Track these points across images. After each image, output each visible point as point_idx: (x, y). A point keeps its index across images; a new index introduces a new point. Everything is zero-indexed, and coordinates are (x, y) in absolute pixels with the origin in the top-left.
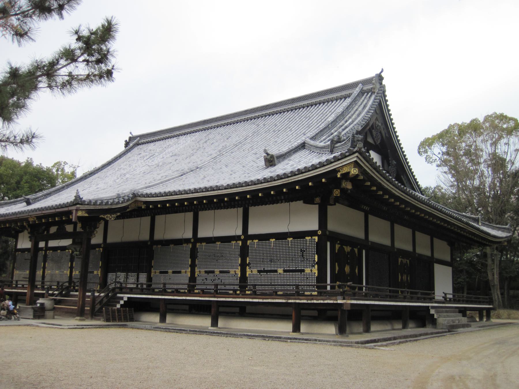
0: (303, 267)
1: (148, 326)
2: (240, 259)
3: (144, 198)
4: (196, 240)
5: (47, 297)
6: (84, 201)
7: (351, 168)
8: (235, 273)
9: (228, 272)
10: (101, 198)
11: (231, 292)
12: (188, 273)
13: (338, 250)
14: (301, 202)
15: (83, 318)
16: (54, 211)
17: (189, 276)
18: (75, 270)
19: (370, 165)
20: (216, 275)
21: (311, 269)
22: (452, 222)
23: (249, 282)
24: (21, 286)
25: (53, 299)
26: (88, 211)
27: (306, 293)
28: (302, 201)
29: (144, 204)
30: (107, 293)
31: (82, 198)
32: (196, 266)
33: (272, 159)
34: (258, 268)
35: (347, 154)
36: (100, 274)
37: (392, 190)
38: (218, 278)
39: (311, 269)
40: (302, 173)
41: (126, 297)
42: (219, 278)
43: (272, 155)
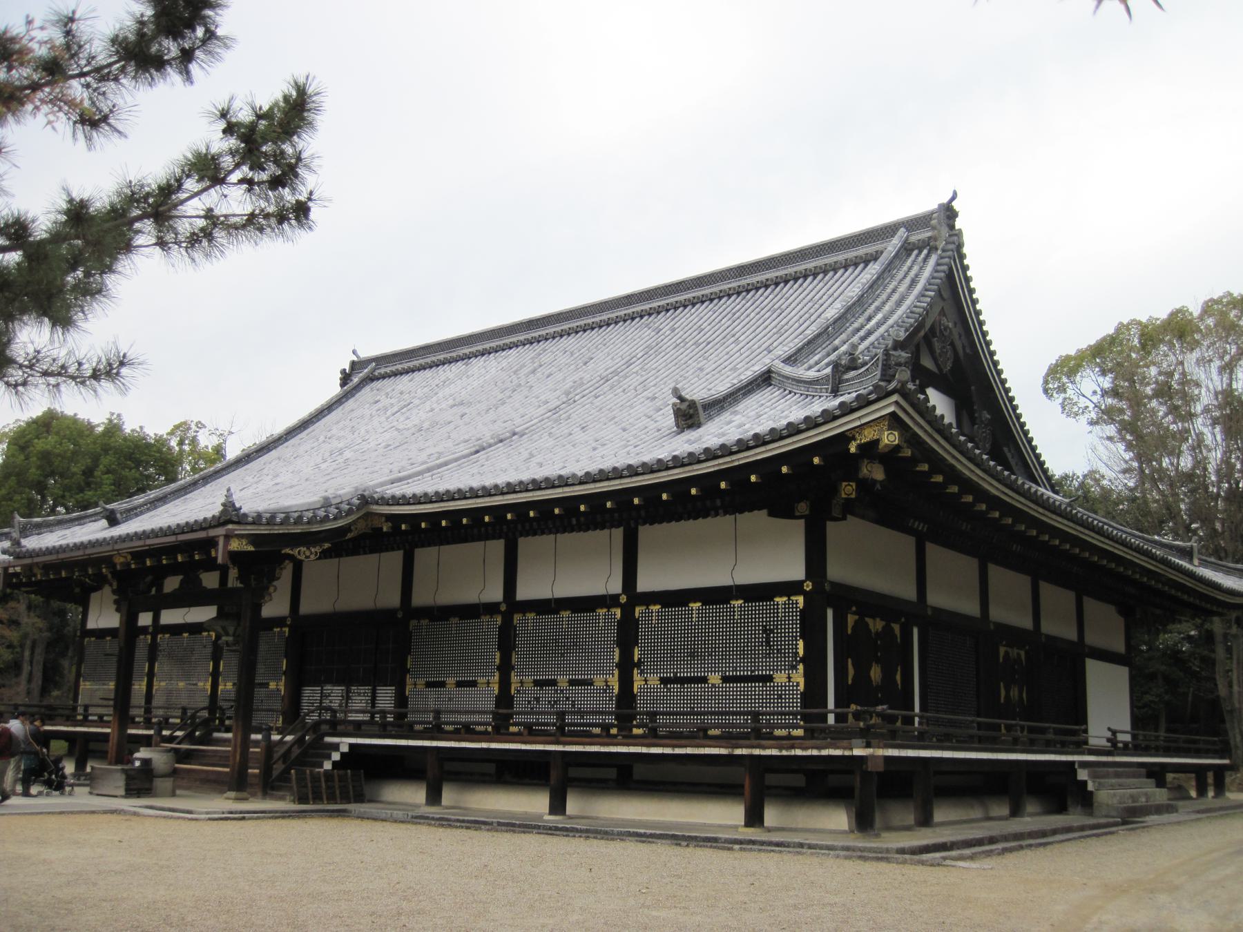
0: (770, 670)
1: (399, 814)
2: (617, 651)
3: (387, 508)
4: (512, 605)
5: (157, 745)
6: (245, 515)
7: (881, 431)
8: (607, 685)
9: (590, 683)
10: (285, 508)
11: (597, 730)
12: (494, 685)
13: (853, 627)
14: (761, 516)
15: (245, 794)
16: (172, 539)
17: (496, 692)
18: (225, 681)
19: (929, 422)
20: (560, 690)
21: (789, 674)
22: (1129, 557)
23: (640, 706)
24: (95, 718)
25: (172, 749)
26: (254, 539)
27: (778, 732)
28: (765, 512)
29: (386, 521)
30: (299, 734)
31: (240, 508)
32: (513, 668)
33: (691, 411)
34: (660, 673)
35: (873, 397)
36: (282, 688)
37: (981, 482)
38: (566, 697)
39: (789, 674)
40: (765, 443)
41: (345, 743)
42: (569, 697)
43: (692, 400)
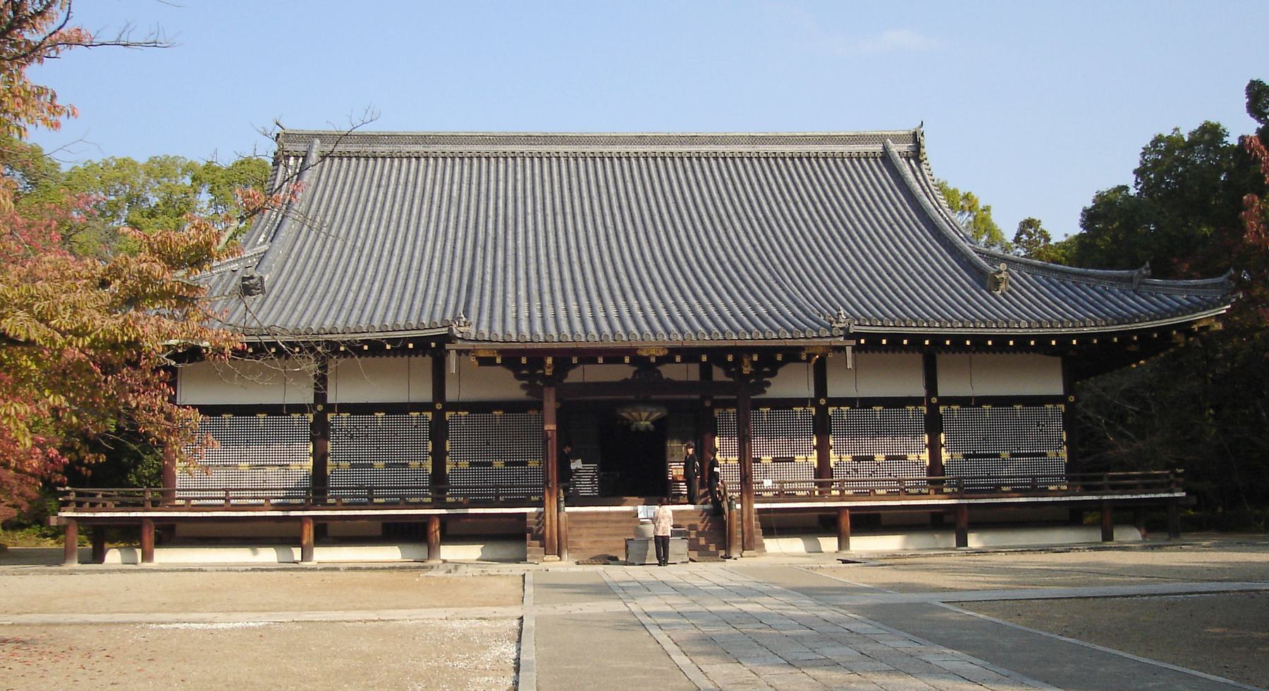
27: (1051, 488)
